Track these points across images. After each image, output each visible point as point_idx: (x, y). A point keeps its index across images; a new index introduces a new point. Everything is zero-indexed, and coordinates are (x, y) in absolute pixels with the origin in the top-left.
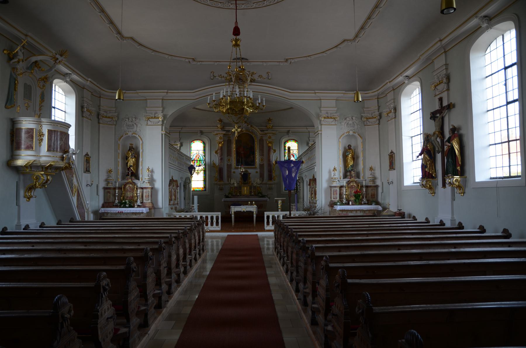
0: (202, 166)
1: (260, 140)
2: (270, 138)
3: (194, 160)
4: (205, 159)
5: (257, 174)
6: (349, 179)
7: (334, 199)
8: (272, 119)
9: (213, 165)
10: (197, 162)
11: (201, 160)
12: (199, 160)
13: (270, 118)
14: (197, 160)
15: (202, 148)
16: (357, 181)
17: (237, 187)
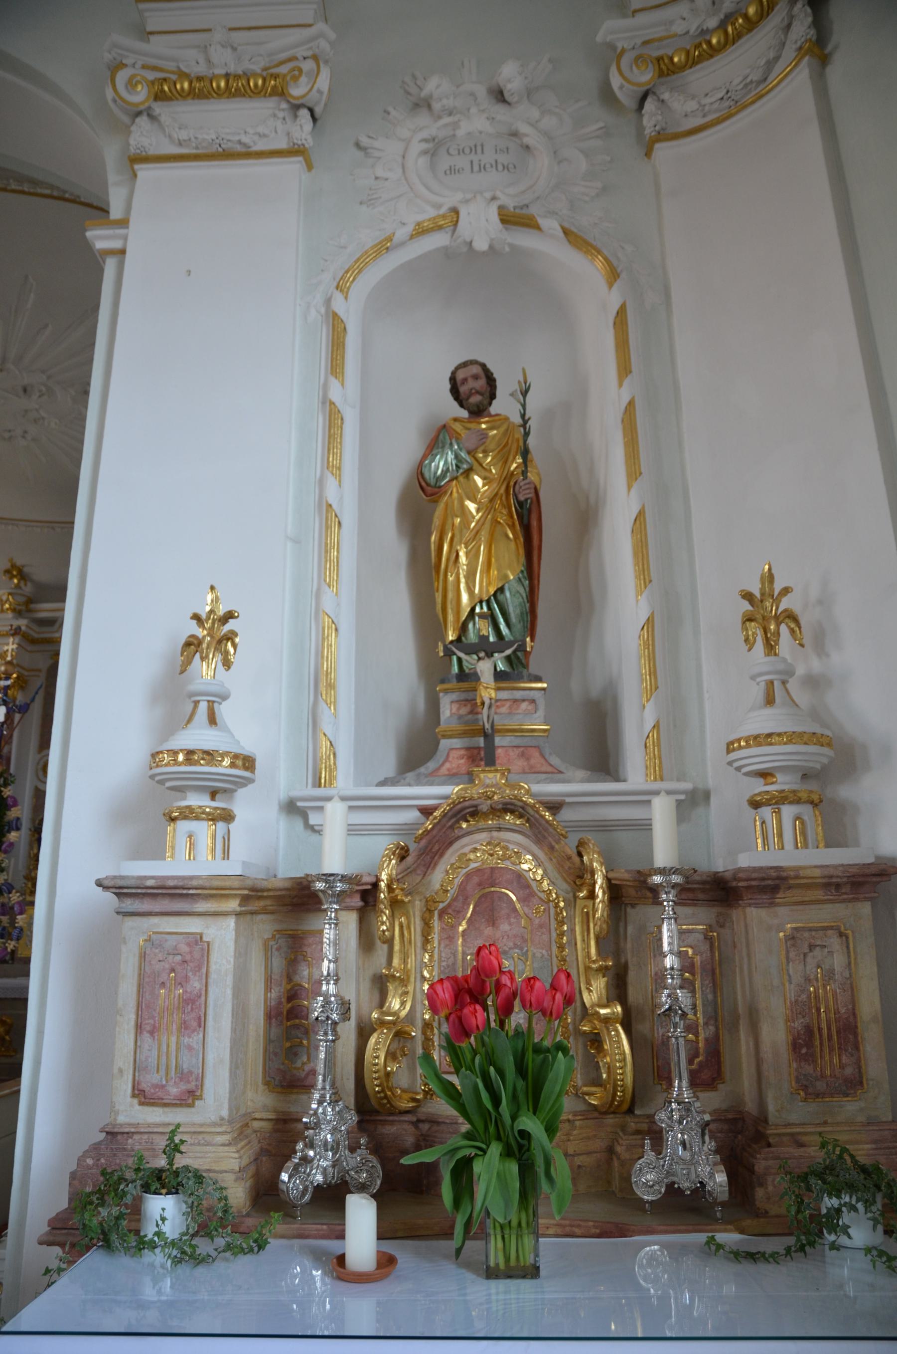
6: (452, 777)
7: (142, 1096)
16: (555, 807)
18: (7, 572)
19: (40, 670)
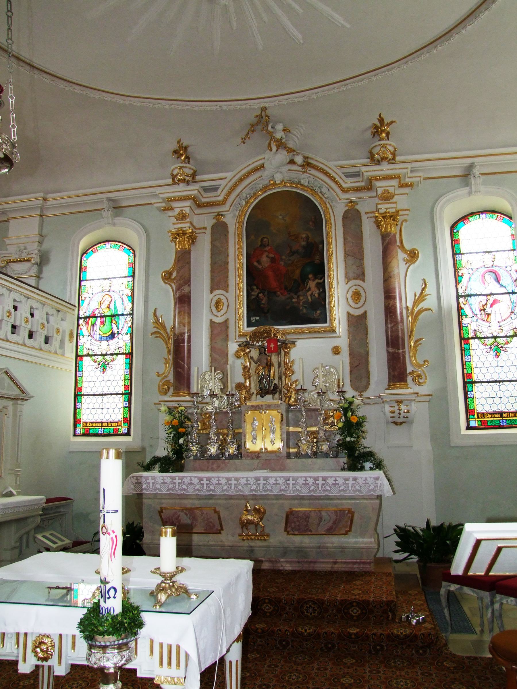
0: (120, 336)
1: (345, 217)
2: (387, 197)
3: (94, 316)
4: (132, 309)
5: (337, 356)
8: (392, 122)
9: (155, 329)
10: (102, 323)
11: (118, 315)
12: (109, 314)
13: (381, 120)
14: (105, 316)
15: (125, 271)
17: (227, 413)
18: (175, 152)
19: (206, 228)
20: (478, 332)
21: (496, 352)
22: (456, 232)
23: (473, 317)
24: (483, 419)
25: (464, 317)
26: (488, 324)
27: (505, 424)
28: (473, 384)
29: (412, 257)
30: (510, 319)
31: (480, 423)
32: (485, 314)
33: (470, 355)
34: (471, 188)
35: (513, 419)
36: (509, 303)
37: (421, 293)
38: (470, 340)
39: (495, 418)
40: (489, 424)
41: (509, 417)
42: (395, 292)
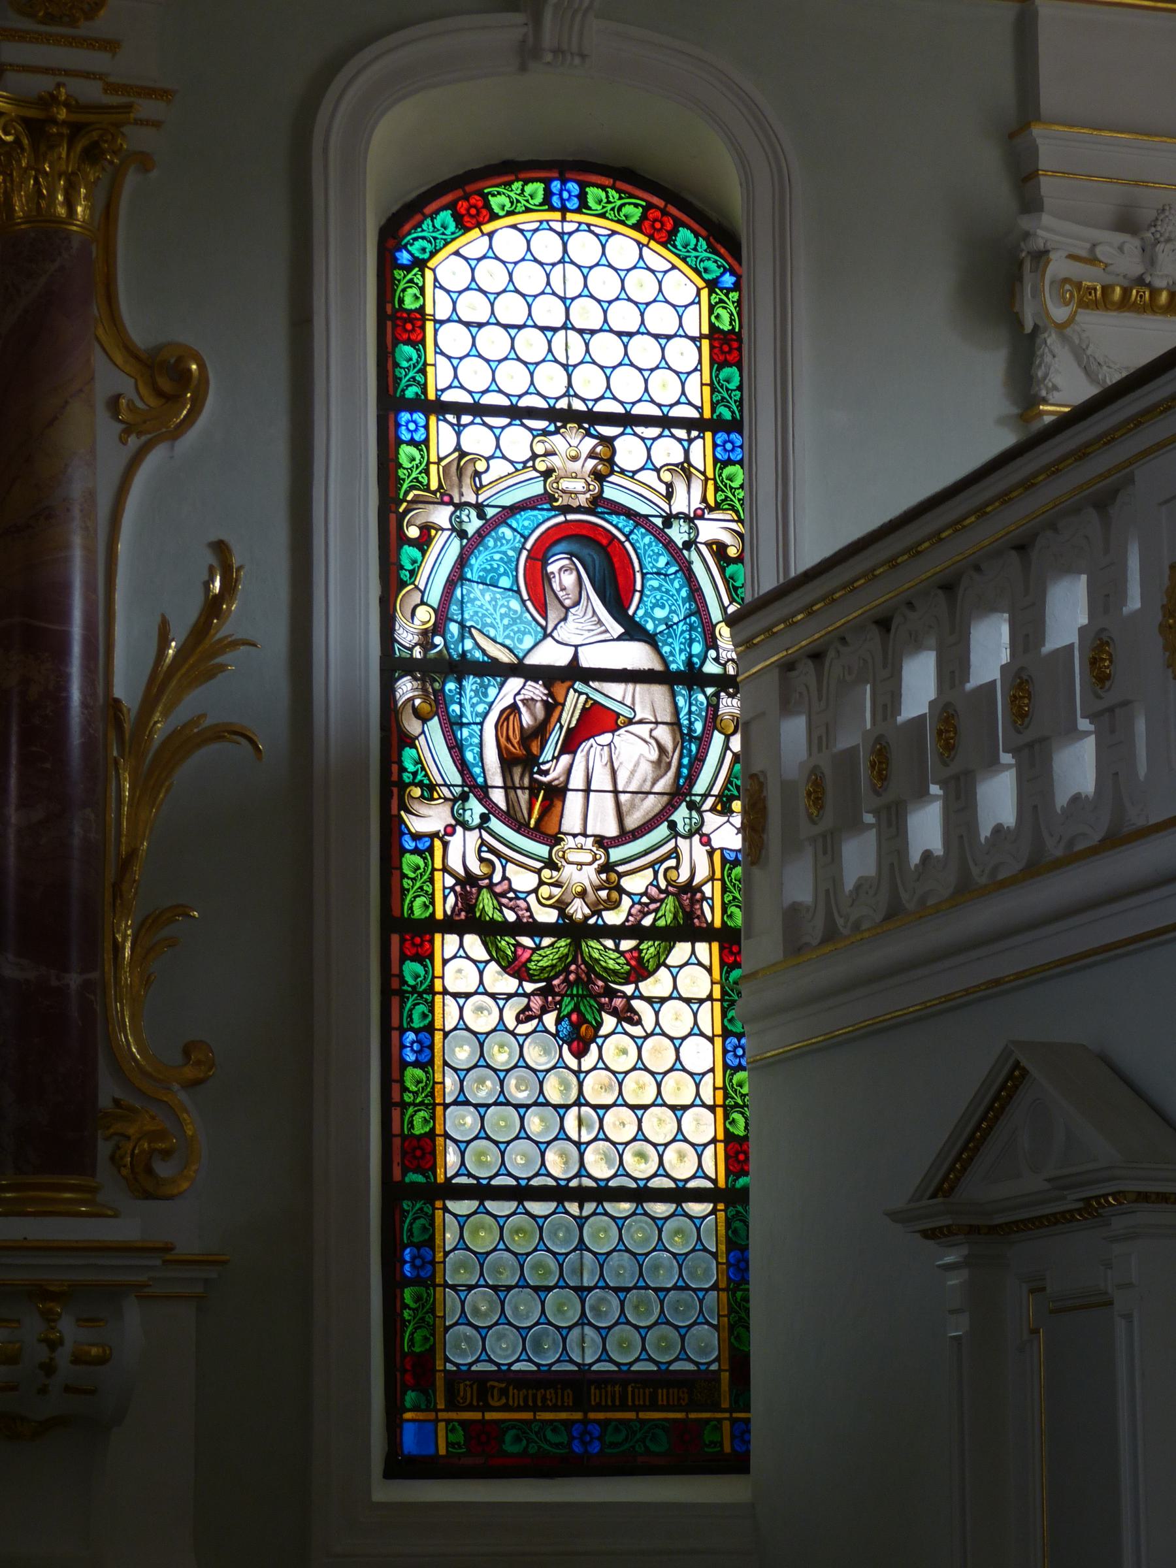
20: (485, 894)
21: (574, 1017)
22: (408, 269)
23: (464, 797)
24: (477, 1416)
25: (417, 792)
26: (542, 850)
27: (595, 1448)
28: (438, 1204)
29: (159, 393)
30: (663, 830)
31: (459, 1436)
32: (534, 788)
33: (430, 1029)
34: (537, 21)
35: (643, 1422)
36: (664, 734)
37: (201, 630)
38: (438, 937)
39: (546, 1409)
40: (510, 1447)
41: (623, 1407)
42: (65, 616)
